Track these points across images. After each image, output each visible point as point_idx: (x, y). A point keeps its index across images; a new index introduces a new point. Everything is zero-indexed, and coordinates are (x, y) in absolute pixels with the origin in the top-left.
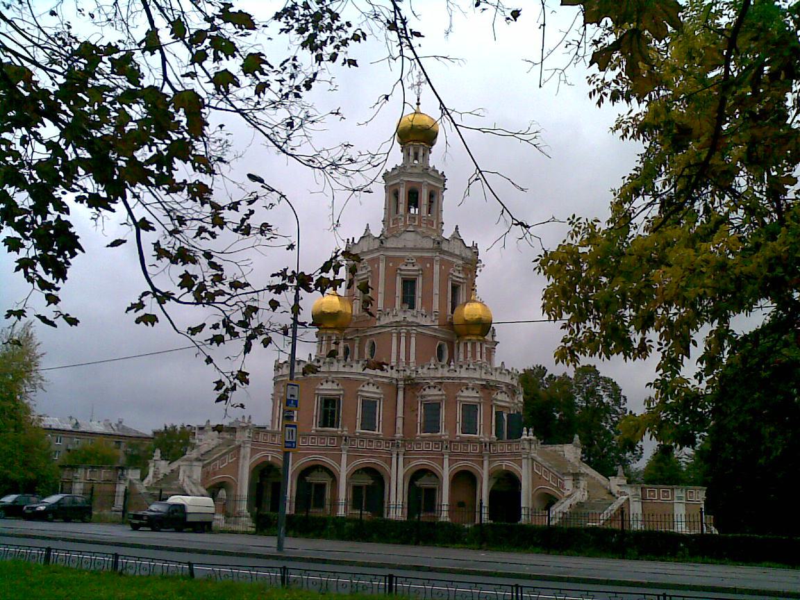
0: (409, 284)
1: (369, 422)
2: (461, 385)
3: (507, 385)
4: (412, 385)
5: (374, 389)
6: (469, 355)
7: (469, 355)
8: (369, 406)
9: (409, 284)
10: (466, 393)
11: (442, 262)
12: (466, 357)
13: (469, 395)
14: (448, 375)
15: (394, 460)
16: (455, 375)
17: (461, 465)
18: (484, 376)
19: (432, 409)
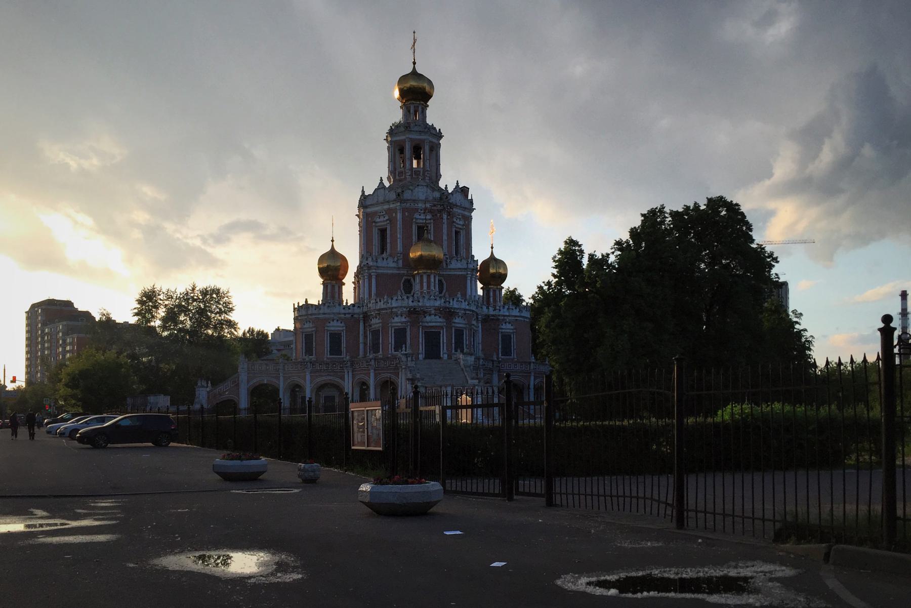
0: (383, 232)
1: (335, 347)
2: (392, 313)
3: (438, 309)
4: (366, 317)
5: (339, 324)
6: (425, 284)
7: (425, 284)
8: (335, 339)
9: (383, 232)
10: (396, 319)
11: (404, 210)
12: (429, 287)
13: (398, 321)
14: (383, 306)
15: (346, 376)
16: (389, 305)
17: (386, 375)
18: (411, 304)
19: (376, 333)
